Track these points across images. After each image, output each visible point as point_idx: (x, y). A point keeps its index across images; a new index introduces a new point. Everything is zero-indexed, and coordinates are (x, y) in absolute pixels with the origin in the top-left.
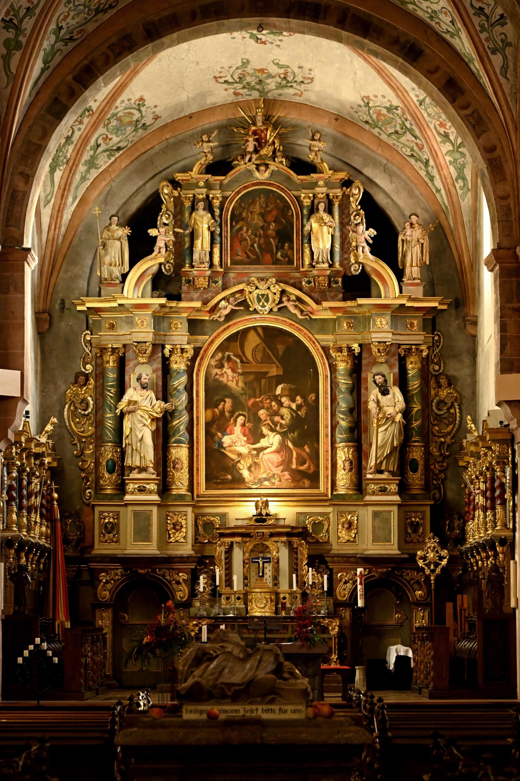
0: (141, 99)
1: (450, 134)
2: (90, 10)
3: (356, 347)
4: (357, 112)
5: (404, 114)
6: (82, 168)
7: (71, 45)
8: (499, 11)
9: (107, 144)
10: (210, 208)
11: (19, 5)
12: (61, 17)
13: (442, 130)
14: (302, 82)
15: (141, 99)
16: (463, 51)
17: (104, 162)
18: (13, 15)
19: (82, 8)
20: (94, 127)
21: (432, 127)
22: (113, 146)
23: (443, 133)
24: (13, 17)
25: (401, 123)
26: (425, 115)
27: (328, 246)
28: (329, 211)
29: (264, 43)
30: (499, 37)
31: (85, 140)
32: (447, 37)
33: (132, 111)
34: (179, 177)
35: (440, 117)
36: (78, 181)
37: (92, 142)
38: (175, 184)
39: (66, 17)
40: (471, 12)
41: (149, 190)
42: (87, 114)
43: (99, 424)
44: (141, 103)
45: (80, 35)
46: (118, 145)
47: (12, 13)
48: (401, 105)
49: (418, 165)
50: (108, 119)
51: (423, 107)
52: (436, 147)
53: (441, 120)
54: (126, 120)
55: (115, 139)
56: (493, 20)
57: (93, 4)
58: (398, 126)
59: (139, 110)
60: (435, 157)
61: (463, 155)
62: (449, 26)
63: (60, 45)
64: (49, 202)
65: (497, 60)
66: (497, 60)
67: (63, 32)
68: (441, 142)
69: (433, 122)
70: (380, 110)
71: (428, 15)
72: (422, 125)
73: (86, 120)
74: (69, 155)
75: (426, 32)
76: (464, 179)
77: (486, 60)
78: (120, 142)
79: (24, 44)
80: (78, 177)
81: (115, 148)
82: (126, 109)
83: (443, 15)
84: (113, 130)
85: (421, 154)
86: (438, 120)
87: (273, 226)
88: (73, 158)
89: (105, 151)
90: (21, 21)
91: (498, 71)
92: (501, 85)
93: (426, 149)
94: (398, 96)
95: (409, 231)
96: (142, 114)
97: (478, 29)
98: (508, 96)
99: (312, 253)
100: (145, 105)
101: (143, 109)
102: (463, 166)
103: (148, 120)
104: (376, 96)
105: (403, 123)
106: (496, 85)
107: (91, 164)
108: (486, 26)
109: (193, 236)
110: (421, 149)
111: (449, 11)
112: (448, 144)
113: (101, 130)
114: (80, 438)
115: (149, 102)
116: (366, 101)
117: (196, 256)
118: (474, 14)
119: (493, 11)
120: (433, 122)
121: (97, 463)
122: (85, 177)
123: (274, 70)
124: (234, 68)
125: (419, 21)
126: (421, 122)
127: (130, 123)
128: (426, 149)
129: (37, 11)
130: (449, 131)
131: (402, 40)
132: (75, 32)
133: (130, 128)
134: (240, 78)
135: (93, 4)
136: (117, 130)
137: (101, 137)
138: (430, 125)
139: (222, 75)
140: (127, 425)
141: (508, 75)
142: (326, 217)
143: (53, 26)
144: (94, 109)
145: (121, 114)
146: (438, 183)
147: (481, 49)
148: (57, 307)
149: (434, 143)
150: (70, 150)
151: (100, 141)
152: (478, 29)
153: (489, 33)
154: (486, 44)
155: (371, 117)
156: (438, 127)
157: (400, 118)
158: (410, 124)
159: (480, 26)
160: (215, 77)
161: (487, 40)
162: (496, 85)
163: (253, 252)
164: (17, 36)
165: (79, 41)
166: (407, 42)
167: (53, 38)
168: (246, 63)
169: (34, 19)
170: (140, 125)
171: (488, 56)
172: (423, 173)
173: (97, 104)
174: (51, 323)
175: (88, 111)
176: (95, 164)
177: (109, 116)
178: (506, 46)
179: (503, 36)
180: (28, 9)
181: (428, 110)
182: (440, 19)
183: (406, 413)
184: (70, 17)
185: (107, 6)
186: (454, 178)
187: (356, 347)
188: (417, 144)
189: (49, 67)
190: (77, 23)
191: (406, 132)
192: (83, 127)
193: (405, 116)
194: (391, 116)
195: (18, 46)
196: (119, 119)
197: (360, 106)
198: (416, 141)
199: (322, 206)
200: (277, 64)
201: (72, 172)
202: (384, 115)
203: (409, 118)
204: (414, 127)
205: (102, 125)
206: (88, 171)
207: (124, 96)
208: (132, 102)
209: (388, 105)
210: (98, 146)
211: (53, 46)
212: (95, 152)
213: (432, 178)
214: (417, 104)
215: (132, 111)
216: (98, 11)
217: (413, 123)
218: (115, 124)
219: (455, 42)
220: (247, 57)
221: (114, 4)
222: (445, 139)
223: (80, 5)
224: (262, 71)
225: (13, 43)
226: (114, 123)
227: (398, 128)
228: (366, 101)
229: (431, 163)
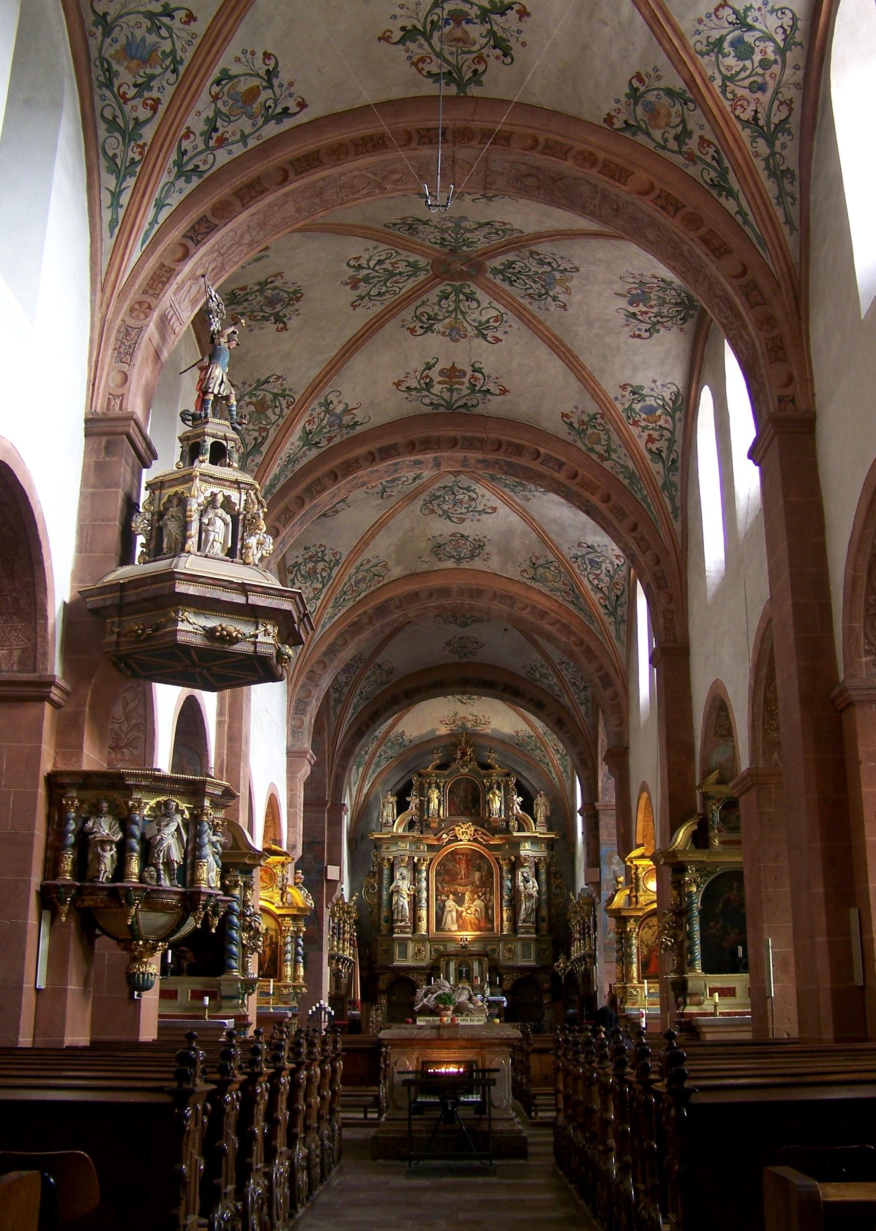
3: (513, 858)
6: (373, 767)
7: (367, 701)
8: (583, 684)
10: (438, 787)
17: (384, 764)
20: (379, 746)
27: (498, 807)
28: (499, 789)
32: (557, 698)
34: (422, 771)
37: (378, 753)
38: (420, 775)
41: (407, 779)
43: (380, 897)
49: (543, 766)
54: (395, 743)
55: (390, 752)
60: (552, 761)
61: (566, 760)
63: (362, 701)
76: (567, 772)
80: (371, 771)
87: (470, 796)
95: (539, 799)
99: (490, 810)
103: (407, 743)
107: (378, 765)
109: (429, 801)
110: (545, 757)
113: (382, 748)
114: (370, 905)
115: (407, 734)
117: (431, 812)
121: (379, 918)
123: (470, 718)
136: (390, 748)
140: (395, 898)
142: (497, 792)
143: (358, 692)
146: (554, 775)
148: (359, 837)
163: (460, 809)
168: (456, 714)
172: (546, 770)
174: (356, 845)
183: (539, 892)
187: (513, 858)
195: (340, 701)
196: (392, 742)
199: (495, 786)
206: (376, 768)
207: (395, 731)
213: (551, 772)
216: (381, 685)
224: (464, 718)
226: (389, 744)
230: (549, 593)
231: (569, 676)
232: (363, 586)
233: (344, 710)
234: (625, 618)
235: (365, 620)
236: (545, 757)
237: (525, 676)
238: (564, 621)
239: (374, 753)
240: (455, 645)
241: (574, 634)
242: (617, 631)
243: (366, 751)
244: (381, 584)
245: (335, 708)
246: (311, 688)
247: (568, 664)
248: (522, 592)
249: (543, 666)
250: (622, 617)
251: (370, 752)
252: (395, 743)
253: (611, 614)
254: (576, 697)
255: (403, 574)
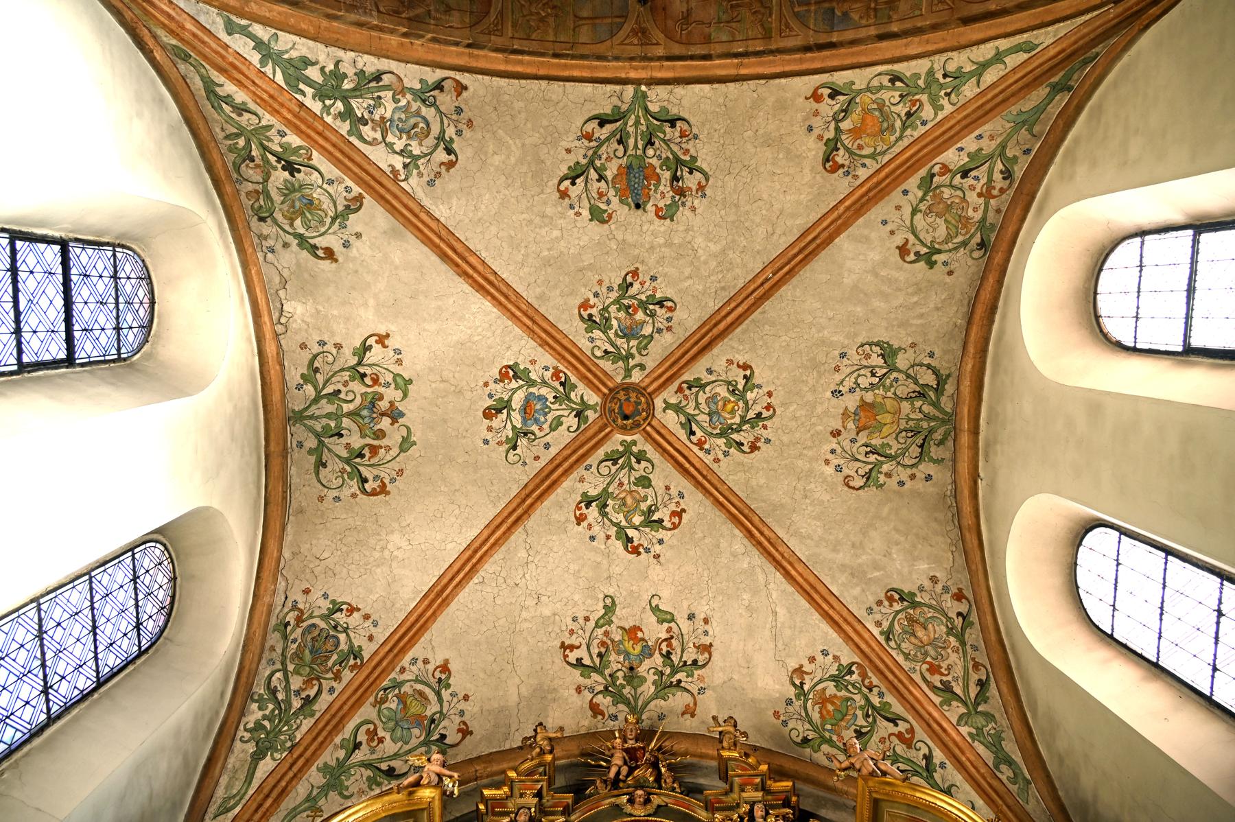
0: (445, 668)
1: (953, 684)
4: (785, 723)
5: (864, 675)
9: (373, 751)
13: (936, 680)
14: (695, 662)
15: (445, 668)
21: (917, 677)
22: (381, 760)
23: (939, 685)
25: (863, 703)
26: (900, 659)
29: (636, 551)
31: (336, 720)
33: (427, 691)
35: (926, 654)
36: (300, 799)
42: (352, 662)
44: (443, 677)
46: (393, 764)
48: (857, 660)
50: (385, 690)
51: (892, 644)
52: (936, 714)
53: (929, 659)
54: (415, 708)
55: (389, 747)
58: (859, 713)
59: (438, 694)
61: (989, 717)
64: (228, 810)
68: (941, 703)
69: (918, 668)
70: (824, 689)
72: (900, 681)
73: (347, 675)
74: (299, 737)
76: (1010, 763)
78: (396, 756)
81: (384, 766)
82: (417, 681)
84: (389, 719)
85: (912, 754)
86: (925, 662)
88: (305, 743)
89: (367, 765)
93: (920, 733)
94: (847, 639)
96: (441, 707)
100: (448, 686)
101: (445, 694)
102: (998, 737)
103: (450, 729)
104: (812, 659)
105: (867, 699)
110: (907, 740)
112: (954, 703)
116: (798, 682)
120: (918, 668)
122: (314, 799)
123: (654, 631)
124: (592, 624)
126: (896, 676)
127: (418, 720)
128: (920, 733)
130: (949, 678)
133: (416, 732)
134: (600, 655)
137: (364, 728)
138: (912, 675)
139: (573, 640)
144: (366, 656)
145: (406, 688)
149: (931, 709)
150: (305, 727)
151: (362, 737)
155: (811, 722)
156: (928, 676)
157: (860, 691)
158: (881, 695)
160: (563, 646)
170: (436, 737)
173: (373, 647)
175: (355, 658)
176: (342, 783)
177: (386, 683)
181: (903, 645)
186: (990, 764)
188: (900, 736)
191: (875, 720)
192: (339, 687)
193: (867, 681)
194: (843, 693)
196: (402, 699)
197: (789, 702)
198: (896, 730)
200: (656, 610)
201: (295, 769)
202: (831, 700)
203: (875, 681)
204: (889, 698)
205: (372, 699)
207: (416, 651)
208: (431, 667)
209: (833, 671)
210: (357, 746)
212: (348, 756)
214: (882, 639)
215: (427, 691)
217: (884, 690)
218: (393, 706)
220: (611, 591)
222: (947, 695)
224: (632, 632)
226: (393, 704)
227: (861, 722)
228: (798, 682)
229: (938, 756)
236: (907, 740)
239: (336, 720)
243: (308, 701)
251: (320, 706)
252: (415, 708)
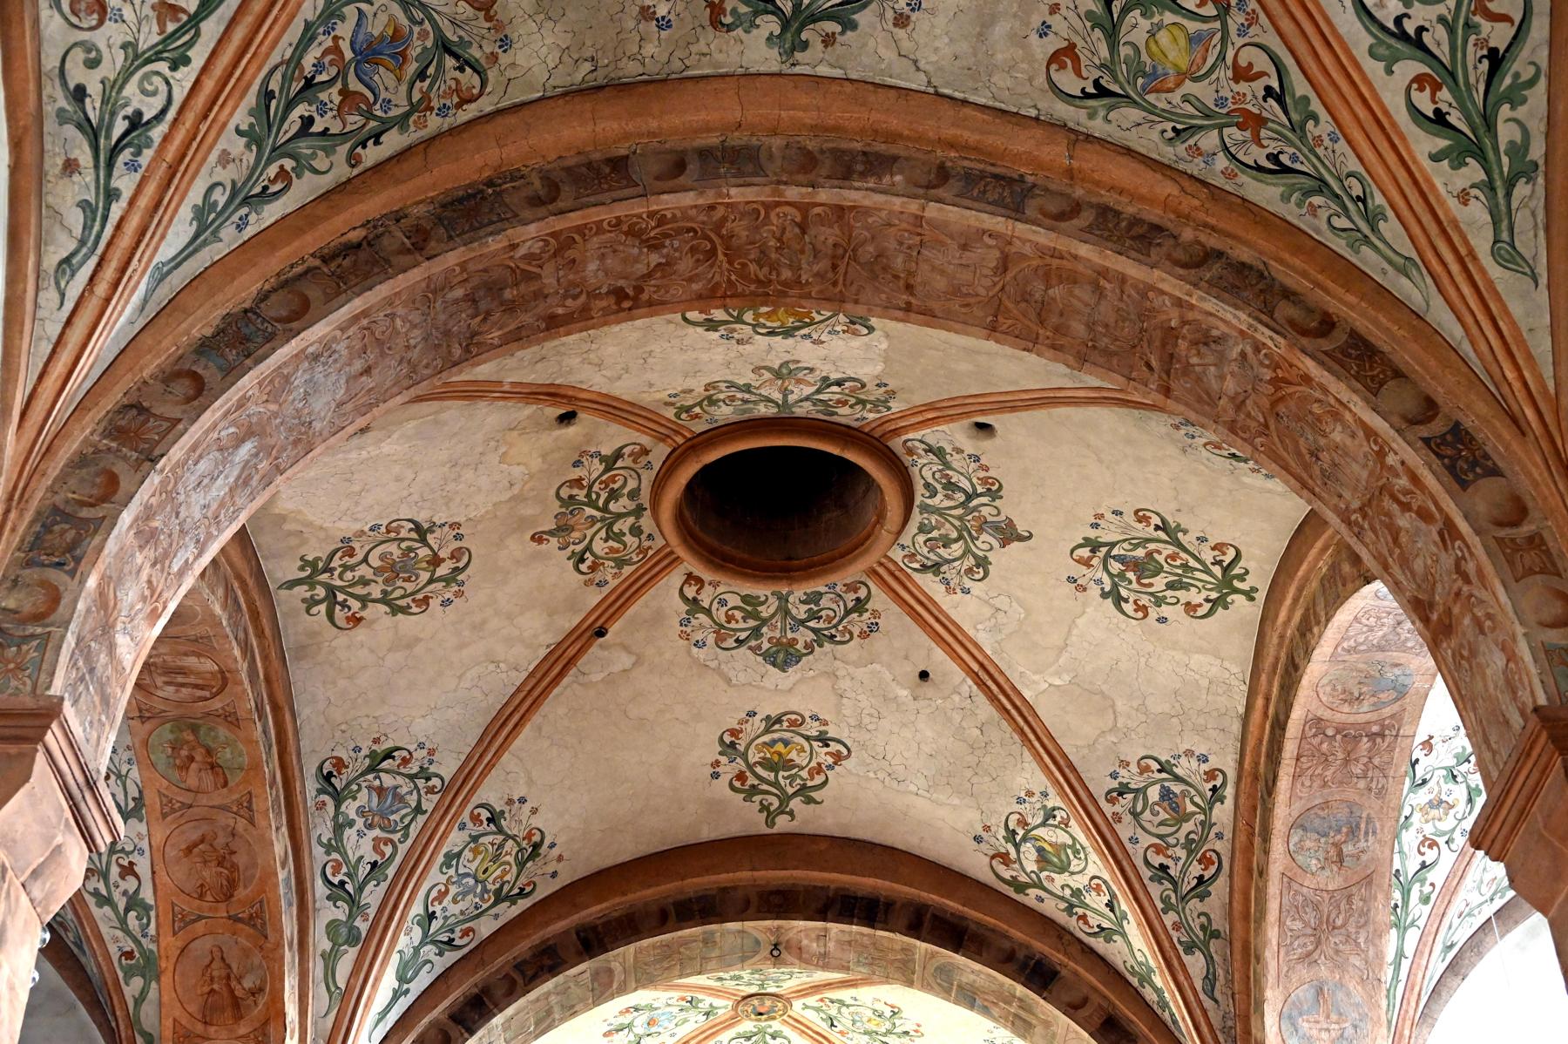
2: (485, 890)
7: (451, 957)
8: (1196, 870)
11: (358, 855)
12: (434, 894)
16: (1131, 962)
18: (345, 874)
19: (471, 881)
24: (346, 879)
30: (1197, 921)
32: (1098, 944)
39: (442, 896)
40: (1146, 873)
45: (466, 940)
47: (344, 870)
56: (1185, 888)
57: (491, 880)
62: (1102, 915)
63: (429, 951)
65: (1195, 964)
66: (1195, 964)
67: (435, 925)
71: (1063, 905)
75: (1060, 937)
77: (1175, 963)
79: (364, 935)
83: (1094, 894)
90: (361, 889)
91: (1198, 985)
92: (1205, 1012)
97: (1160, 906)
98: (1218, 1032)
106: (1198, 1012)
108: (1173, 900)
111: (1105, 882)
118: (1151, 879)
119: (1184, 872)
125: (1046, 924)
129: (391, 872)
131: (1021, 955)
132: (457, 934)
135: (491, 880)
141: (1217, 994)
143: (417, 909)
147: (1166, 944)
152: (1160, 906)
153: (1178, 914)
154: (1175, 935)
159: (1163, 901)
161: (1176, 926)
162: (1198, 1012)
164: (351, 916)
165: (465, 950)
166: (1029, 958)
167: (417, 933)
169: (384, 886)
171: (1179, 958)
178: (1210, 938)
179: (1203, 919)
180: (374, 865)
182: (1087, 906)
184: (449, 897)
185: (516, 891)
189: (407, 991)
190: (462, 913)
195: (353, 938)
211: (417, 950)
216: (499, 897)
219: (1114, 951)
221: (528, 889)
223: (467, 875)
225: (344, 931)
230: (1168, 153)
231: (1146, 840)
232: (392, 90)
233: (363, 972)
234: (1537, 152)
235: (398, 237)
237: (986, 877)
238: (1244, 254)
240: (754, 756)
241: (1288, 294)
242: (1500, 217)
244: (471, 111)
245: (330, 959)
246: (120, 468)
247: (1141, 792)
248: (1055, 153)
249: (1050, 814)
250: (1518, 150)
253: (1467, 148)
254: (1170, 919)
255: (561, 80)
